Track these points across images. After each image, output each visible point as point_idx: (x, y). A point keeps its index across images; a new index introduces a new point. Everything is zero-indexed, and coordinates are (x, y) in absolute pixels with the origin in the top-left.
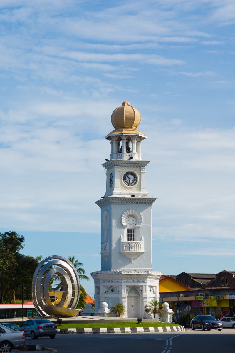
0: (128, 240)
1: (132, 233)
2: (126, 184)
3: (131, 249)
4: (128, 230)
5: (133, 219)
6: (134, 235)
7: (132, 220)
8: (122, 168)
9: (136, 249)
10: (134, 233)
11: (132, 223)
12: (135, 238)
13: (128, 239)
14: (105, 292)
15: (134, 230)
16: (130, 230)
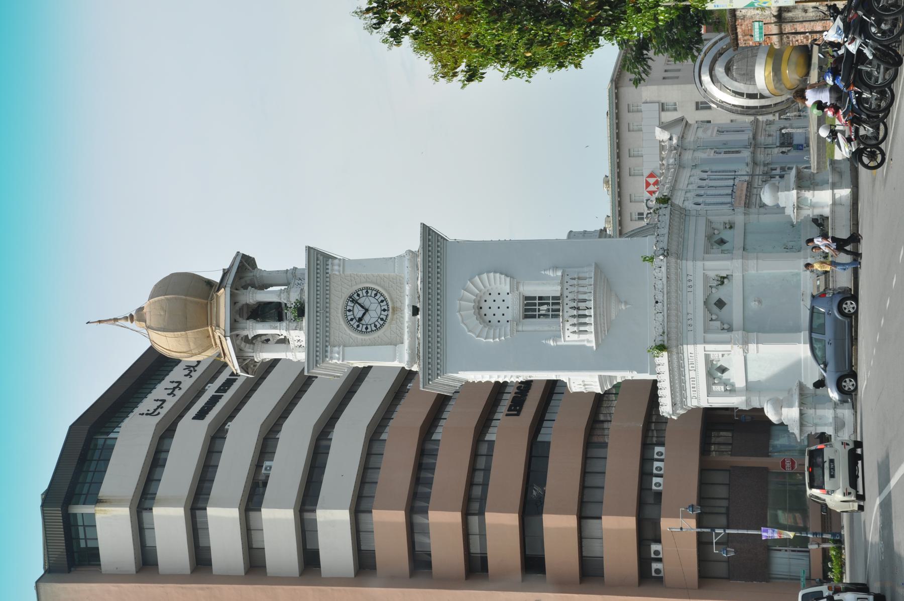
0: (557, 316)
1: (535, 304)
2: (382, 322)
3: (587, 320)
4: (526, 317)
5: (490, 303)
6: (540, 298)
7: (494, 310)
8: (332, 331)
9: (585, 293)
10: (534, 298)
11: (503, 306)
12: (551, 295)
13: (554, 316)
14: (728, 393)
15: (527, 298)
16: (526, 310)
